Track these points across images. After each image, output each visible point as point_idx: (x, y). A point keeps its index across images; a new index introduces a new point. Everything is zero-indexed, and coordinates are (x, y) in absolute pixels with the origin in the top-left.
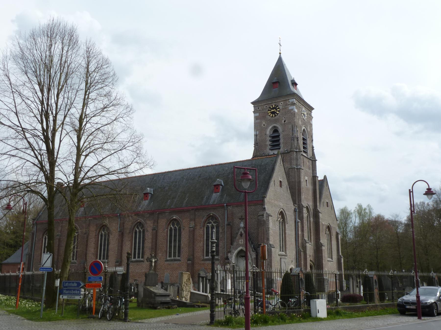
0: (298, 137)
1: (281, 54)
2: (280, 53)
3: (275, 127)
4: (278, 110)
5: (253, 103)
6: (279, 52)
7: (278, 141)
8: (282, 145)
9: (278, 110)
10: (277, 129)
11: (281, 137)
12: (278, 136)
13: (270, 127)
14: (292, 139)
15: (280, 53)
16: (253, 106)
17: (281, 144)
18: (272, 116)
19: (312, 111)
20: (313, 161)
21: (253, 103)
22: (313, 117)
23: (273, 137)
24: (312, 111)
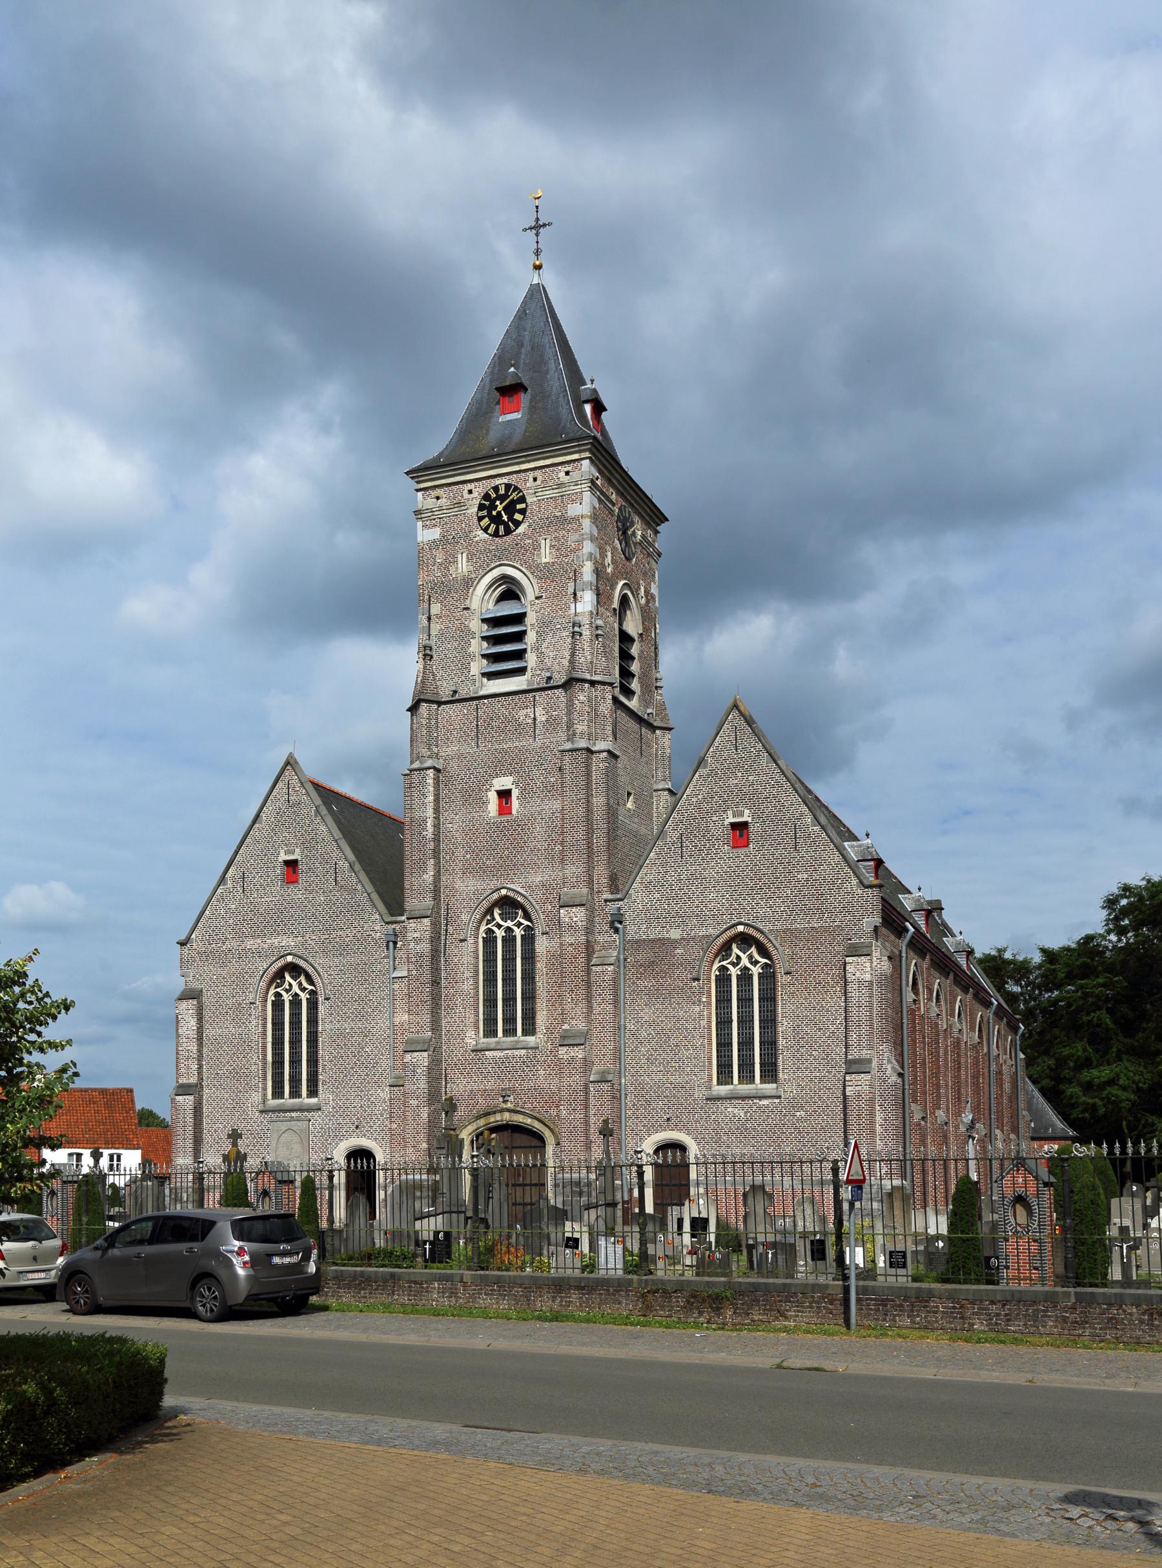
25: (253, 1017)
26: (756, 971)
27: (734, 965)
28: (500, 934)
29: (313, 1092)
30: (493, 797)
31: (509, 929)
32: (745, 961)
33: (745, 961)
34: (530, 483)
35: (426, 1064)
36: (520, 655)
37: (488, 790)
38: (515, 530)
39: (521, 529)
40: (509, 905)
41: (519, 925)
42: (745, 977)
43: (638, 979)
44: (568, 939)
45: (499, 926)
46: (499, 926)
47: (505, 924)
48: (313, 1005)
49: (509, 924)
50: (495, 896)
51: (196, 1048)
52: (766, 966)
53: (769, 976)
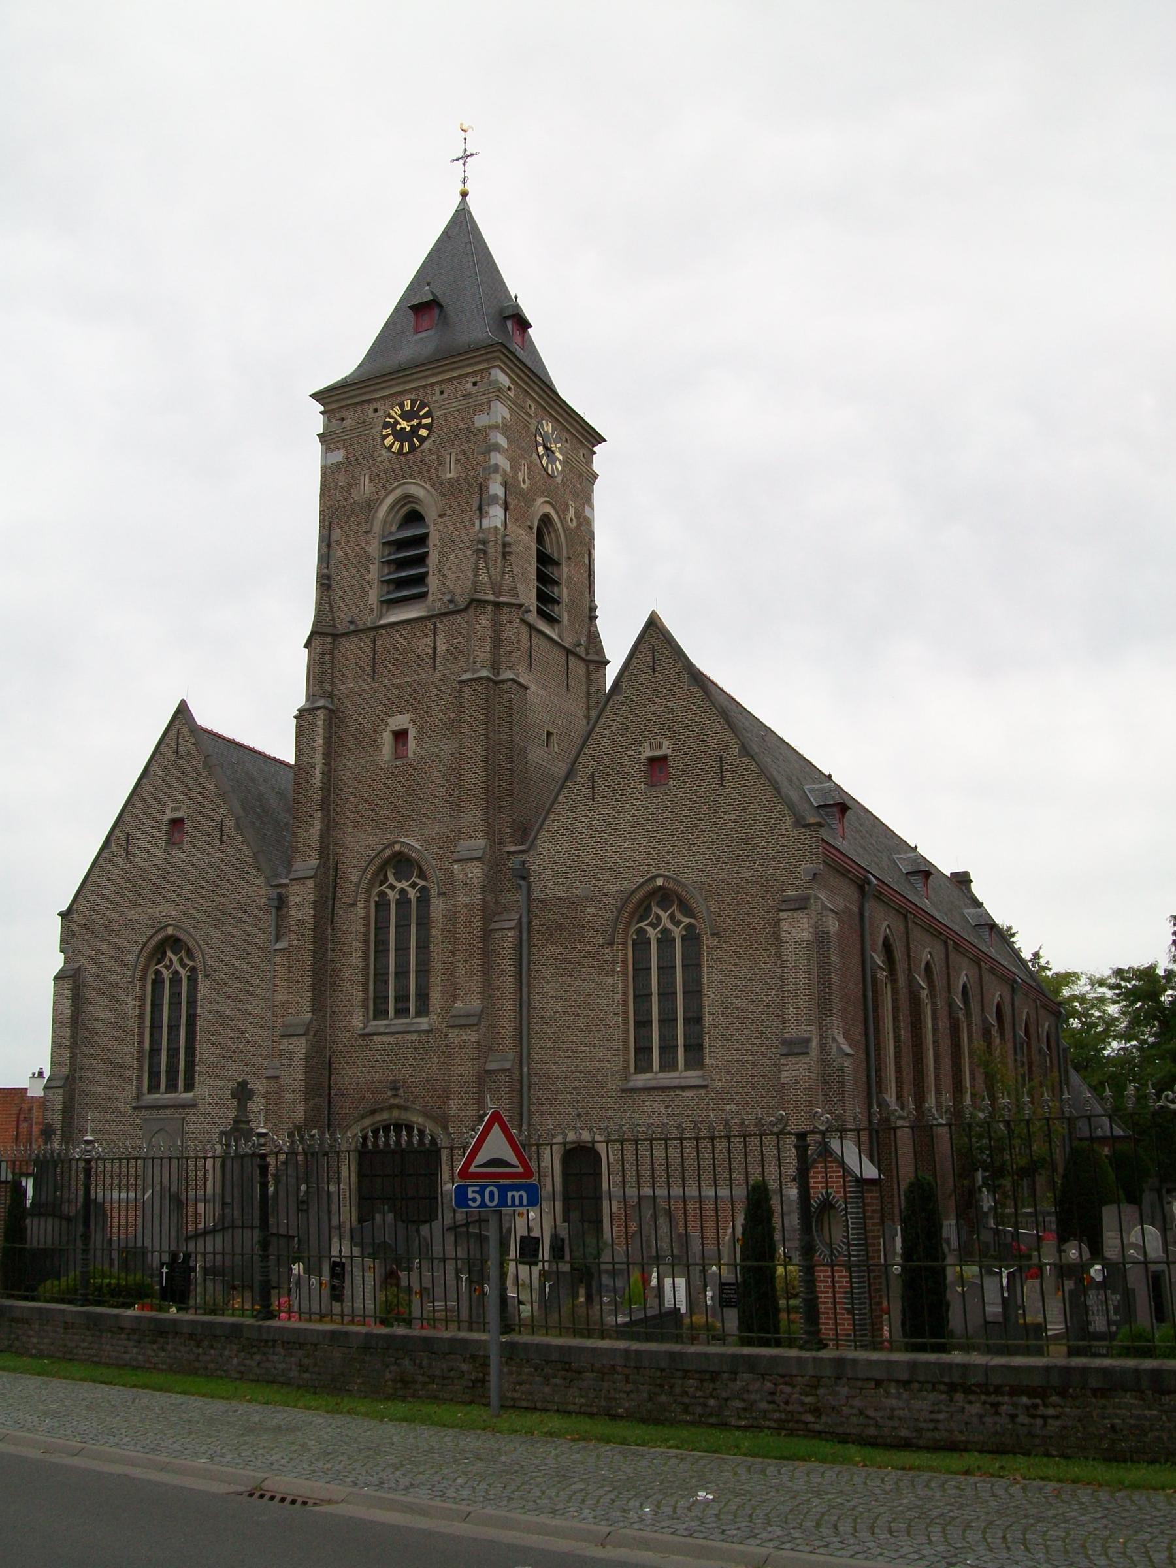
0: (508, 539)
1: (467, 198)
2: (464, 194)
3: (407, 498)
4: (424, 422)
5: (318, 396)
6: (460, 187)
7: (421, 560)
8: (433, 582)
9: (424, 422)
10: (418, 507)
11: (434, 540)
12: (422, 540)
13: (390, 500)
14: (481, 547)
15: (464, 194)
16: (322, 409)
17: (431, 573)
18: (401, 447)
19: (595, 449)
20: (592, 667)
21: (318, 396)
22: (595, 476)
23: (401, 544)
24: (595, 449)
25: (130, 998)
26: (677, 932)
27: (654, 925)
28: (392, 896)
29: (189, 1087)
30: (387, 737)
31: (403, 891)
32: (666, 922)
33: (666, 922)
34: (437, 397)
35: (303, 1051)
36: (421, 579)
37: (383, 731)
38: (419, 446)
39: (426, 445)
40: (402, 863)
41: (413, 885)
42: (666, 940)
43: (543, 945)
44: (463, 899)
45: (392, 887)
46: (392, 887)
47: (399, 885)
48: (193, 980)
49: (404, 885)
50: (388, 852)
51: (69, 1034)
52: (689, 927)
53: (692, 938)
